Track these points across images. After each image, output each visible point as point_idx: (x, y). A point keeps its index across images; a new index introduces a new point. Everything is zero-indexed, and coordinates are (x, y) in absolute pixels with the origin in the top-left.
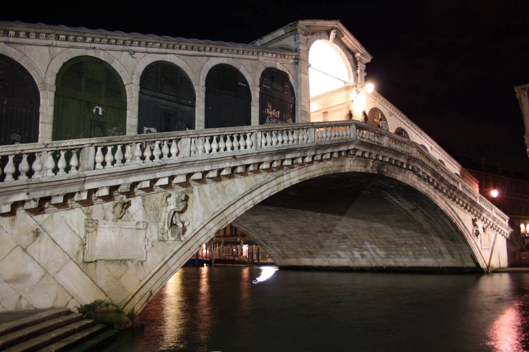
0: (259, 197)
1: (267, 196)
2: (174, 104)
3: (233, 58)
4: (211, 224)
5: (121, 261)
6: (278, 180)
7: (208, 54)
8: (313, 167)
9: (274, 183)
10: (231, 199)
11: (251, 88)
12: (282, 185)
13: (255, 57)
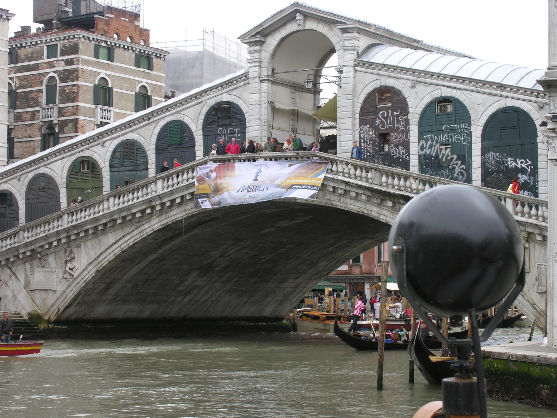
0: (125, 245)
1: (132, 243)
2: (133, 172)
3: (178, 112)
4: (91, 267)
5: (46, 290)
6: (140, 229)
7: (155, 119)
8: (174, 212)
9: (136, 232)
10: (104, 248)
11: (194, 134)
12: (145, 233)
13: (200, 100)
